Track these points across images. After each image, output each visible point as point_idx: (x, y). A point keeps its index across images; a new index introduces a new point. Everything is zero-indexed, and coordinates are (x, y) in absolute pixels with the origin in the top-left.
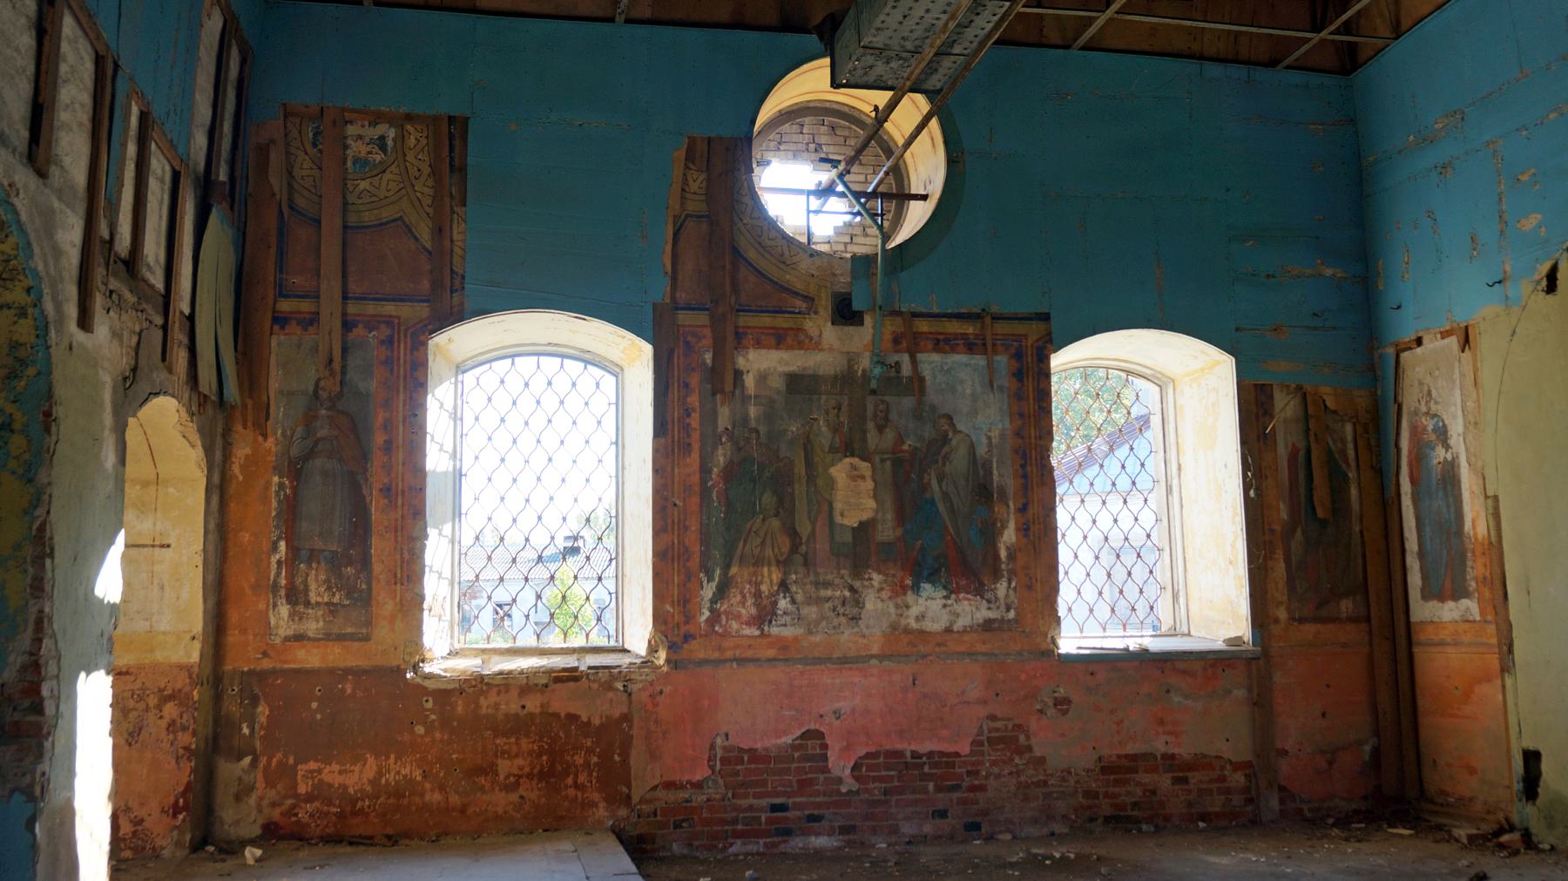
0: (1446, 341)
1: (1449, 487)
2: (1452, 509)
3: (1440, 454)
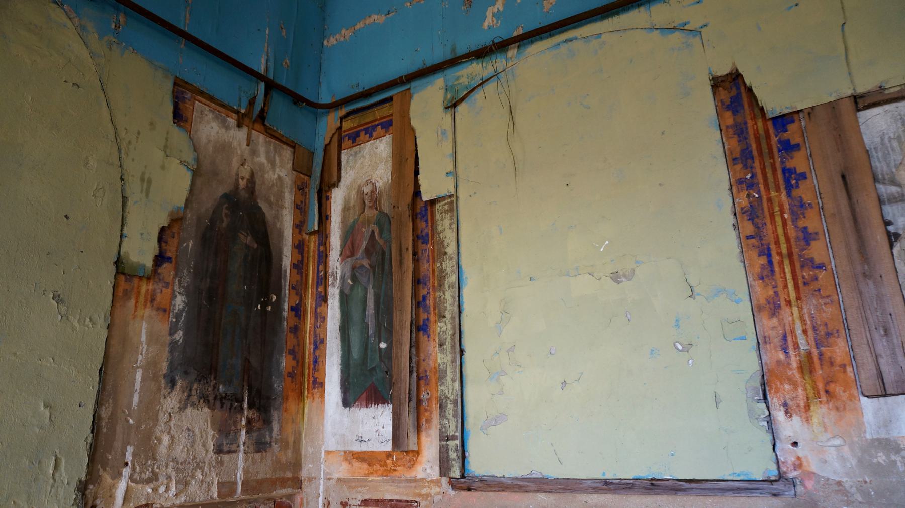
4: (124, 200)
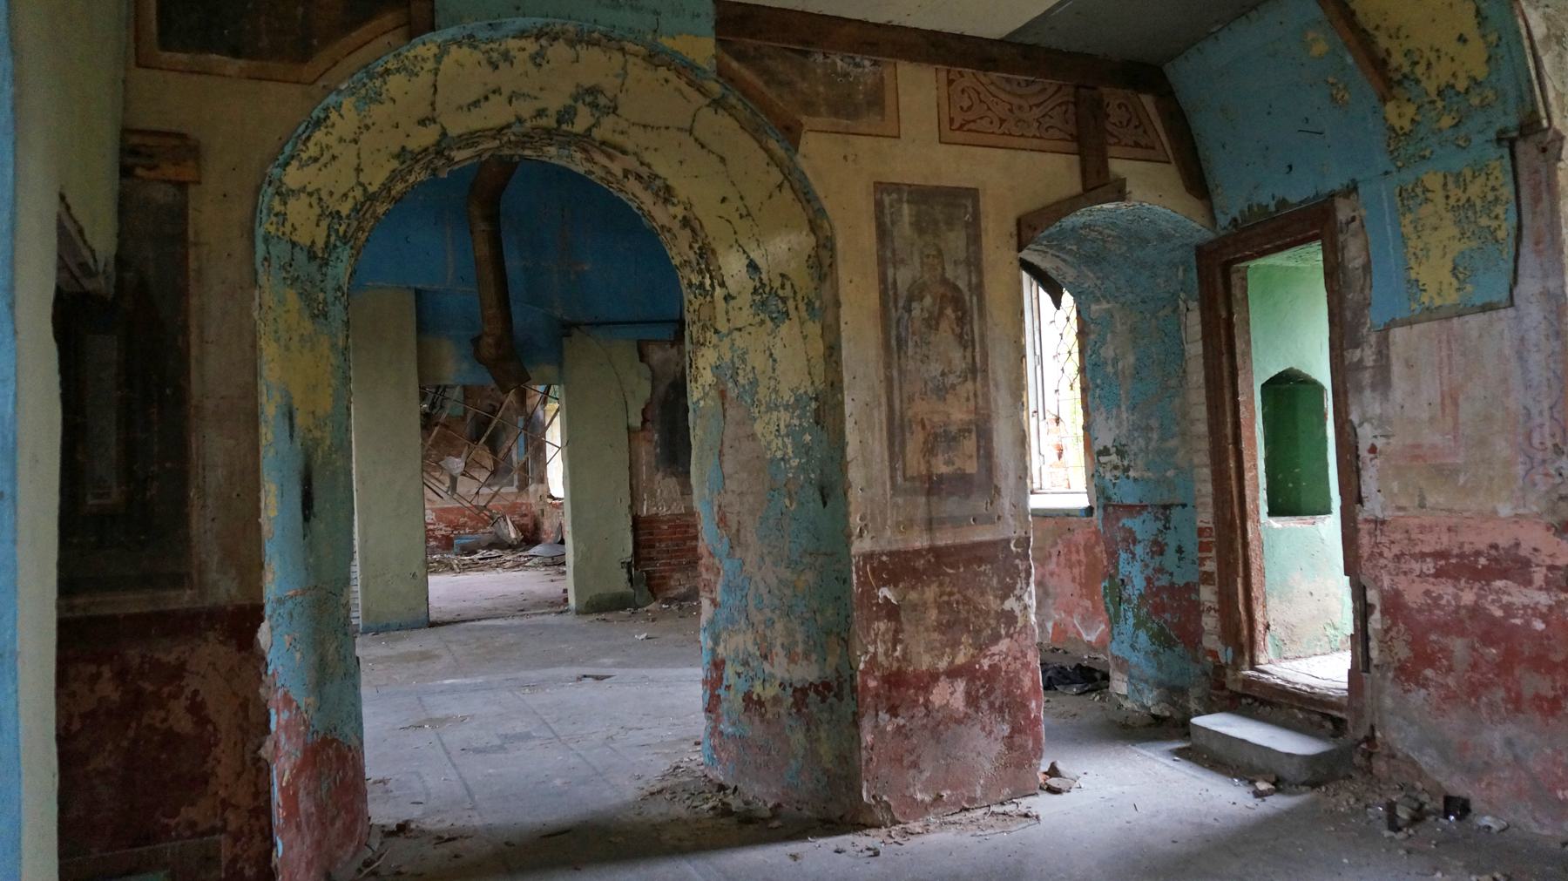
4: (626, 402)
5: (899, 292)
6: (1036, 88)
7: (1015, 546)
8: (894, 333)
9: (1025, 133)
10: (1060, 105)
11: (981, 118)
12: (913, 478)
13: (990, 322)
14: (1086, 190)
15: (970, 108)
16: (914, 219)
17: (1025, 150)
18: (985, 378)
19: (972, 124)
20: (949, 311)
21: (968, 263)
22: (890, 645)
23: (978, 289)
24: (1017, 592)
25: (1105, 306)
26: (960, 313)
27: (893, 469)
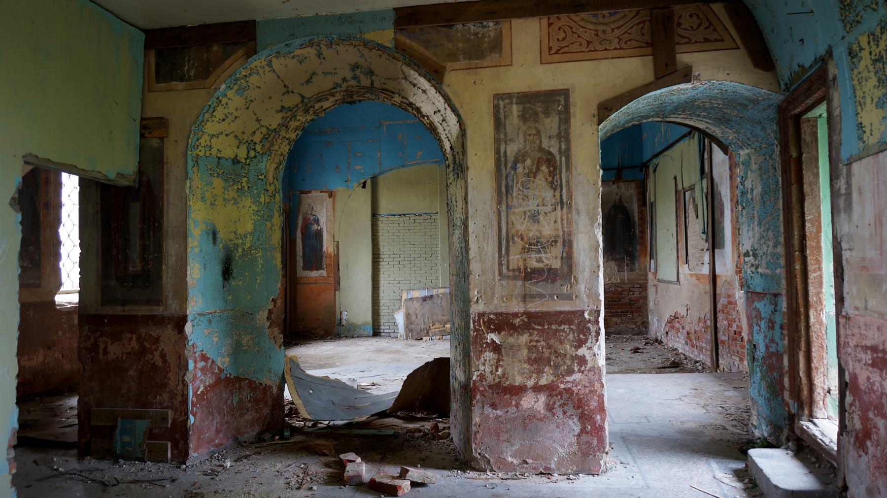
0: (322, 194)
1: (318, 237)
2: (319, 244)
3: (315, 227)
5: (508, 158)
6: (618, 16)
7: (589, 314)
8: (504, 183)
9: (607, 48)
10: (637, 24)
11: (573, 43)
12: (514, 270)
13: (574, 173)
14: (657, 78)
15: (564, 39)
16: (520, 113)
17: (607, 59)
18: (570, 207)
19: (566, 48)
20: (544, 168)
21: (559, 136)
22: (494, 367)
23: (567, 153)
24: (589, 344)
25: (747, 151)
26: (552, 169)
27: (500, 265)
